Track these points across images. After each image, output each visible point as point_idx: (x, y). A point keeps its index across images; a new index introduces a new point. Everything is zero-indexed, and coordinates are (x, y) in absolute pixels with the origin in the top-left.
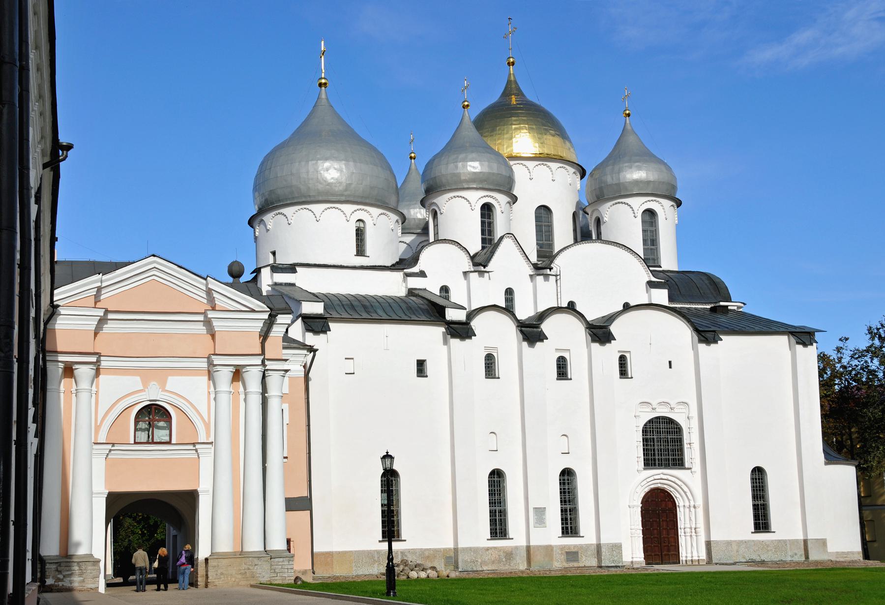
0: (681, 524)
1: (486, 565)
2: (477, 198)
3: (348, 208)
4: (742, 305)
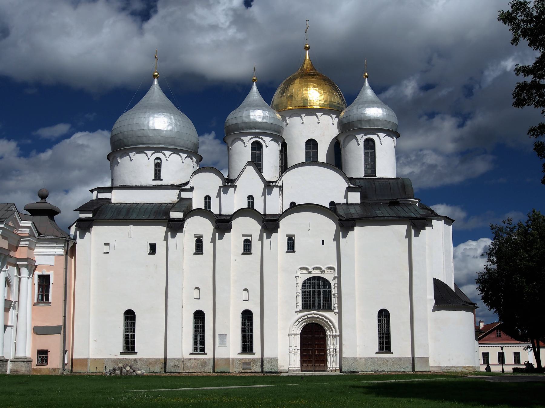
0: (328, 348)
1: (188, 369)
2: (249, 140)
3: (149, 153)
4: (417, 200)
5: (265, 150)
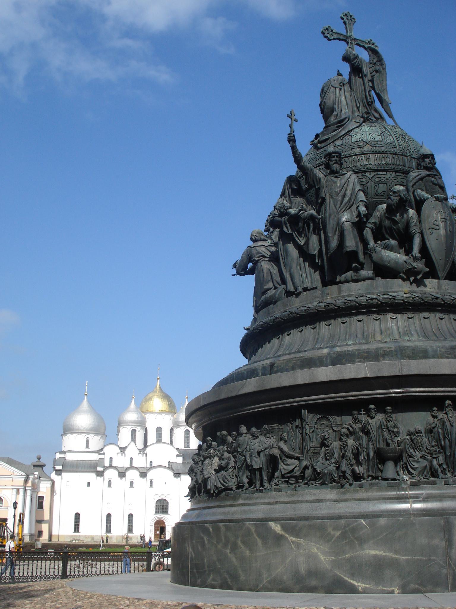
3: (84, 435)
5: (137, 433)
